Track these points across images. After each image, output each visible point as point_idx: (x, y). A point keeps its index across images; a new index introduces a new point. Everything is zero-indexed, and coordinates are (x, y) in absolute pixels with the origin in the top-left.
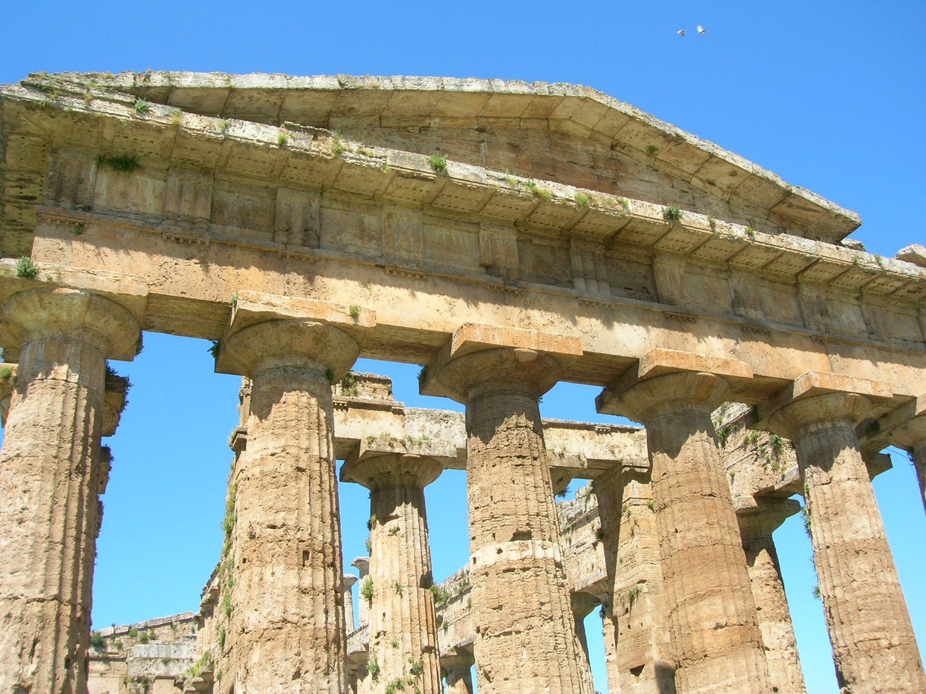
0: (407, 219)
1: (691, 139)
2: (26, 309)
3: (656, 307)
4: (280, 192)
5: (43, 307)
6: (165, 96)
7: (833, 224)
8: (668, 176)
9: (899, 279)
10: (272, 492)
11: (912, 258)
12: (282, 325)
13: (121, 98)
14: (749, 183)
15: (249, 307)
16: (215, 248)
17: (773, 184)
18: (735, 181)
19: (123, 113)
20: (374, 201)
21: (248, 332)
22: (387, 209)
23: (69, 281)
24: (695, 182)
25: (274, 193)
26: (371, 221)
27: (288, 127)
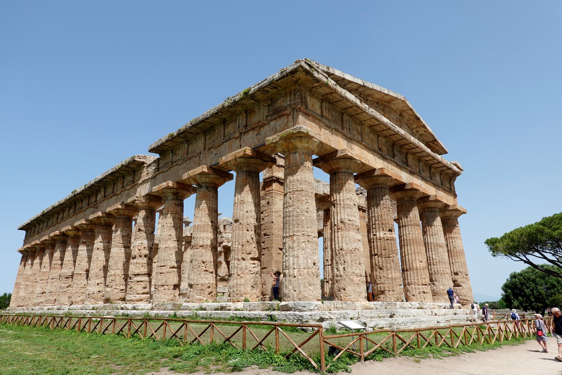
0: (367, 130)
1: (421, 119)
2: (301, 142)
3: (409, 168)
4: (345, 115)
5: (307, 143)
6: (330, 75)
7: (441, 151)
8: (409, 127)
9: (453, 171)
10: (349, 210)
11: (456, 165)
12: (353, 161)
13: (325, 75)
14: (428, 135)
15: (348, 154)
16: (334, 130)
17: (434, 136)
18: (424, 133)
19: (324, 80)
20: (361, 123)
21: (342, 160)
22: (364, 126)
23: (316, 137)
24: (414, 130)
25: (343, 114)
26: (359, 128)
27: (356, 96)
